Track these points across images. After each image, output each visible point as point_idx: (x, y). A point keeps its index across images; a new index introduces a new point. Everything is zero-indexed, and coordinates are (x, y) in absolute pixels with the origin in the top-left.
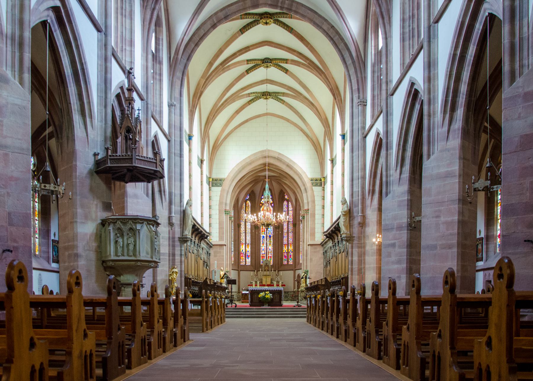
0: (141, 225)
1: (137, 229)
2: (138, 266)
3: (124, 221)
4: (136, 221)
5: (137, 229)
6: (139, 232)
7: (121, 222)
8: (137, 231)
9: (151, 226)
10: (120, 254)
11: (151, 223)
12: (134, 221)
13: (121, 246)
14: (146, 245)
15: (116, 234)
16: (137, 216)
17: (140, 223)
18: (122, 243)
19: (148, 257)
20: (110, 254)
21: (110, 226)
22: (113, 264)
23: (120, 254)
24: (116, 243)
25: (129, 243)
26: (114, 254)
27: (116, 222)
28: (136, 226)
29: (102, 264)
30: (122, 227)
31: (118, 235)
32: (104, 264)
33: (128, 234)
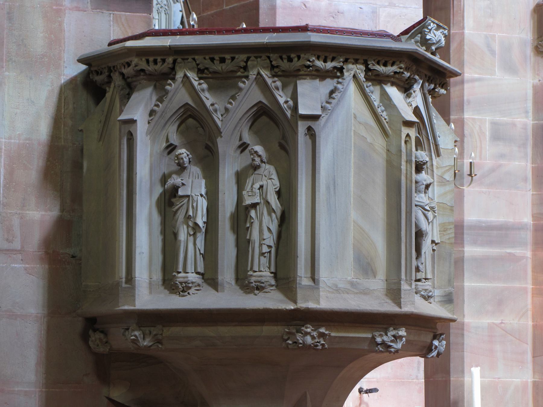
0: (329, 84)
1: (302, 111)
2: (306, 347)
3: (217, 67)
4: (297, 63)
5: (302, 111)
6: (311, 133)
7: (201, 72)
8: (302, 127)
9: (393, 92)
10: (192, 277)
11: (390, 70)
12: (285, 65)
13: (201, 221)
14: (353, 215)
15: (171, 148)
16: (304, 29)
17: (322, 75)
18: (203, 204)
19: (366, 292)
20: (130, 278)
21: (135, 96)
22: (146, 343)
23: (192, 277)
24: (171, 204)
25: (248, 201)
26: (158, 276)
27: (170, 74)
28: (294, 97)
29: (85, 337)
30: (208, 99)
31: (183, 152)
32: (95, 337)
33: (243, 147)
